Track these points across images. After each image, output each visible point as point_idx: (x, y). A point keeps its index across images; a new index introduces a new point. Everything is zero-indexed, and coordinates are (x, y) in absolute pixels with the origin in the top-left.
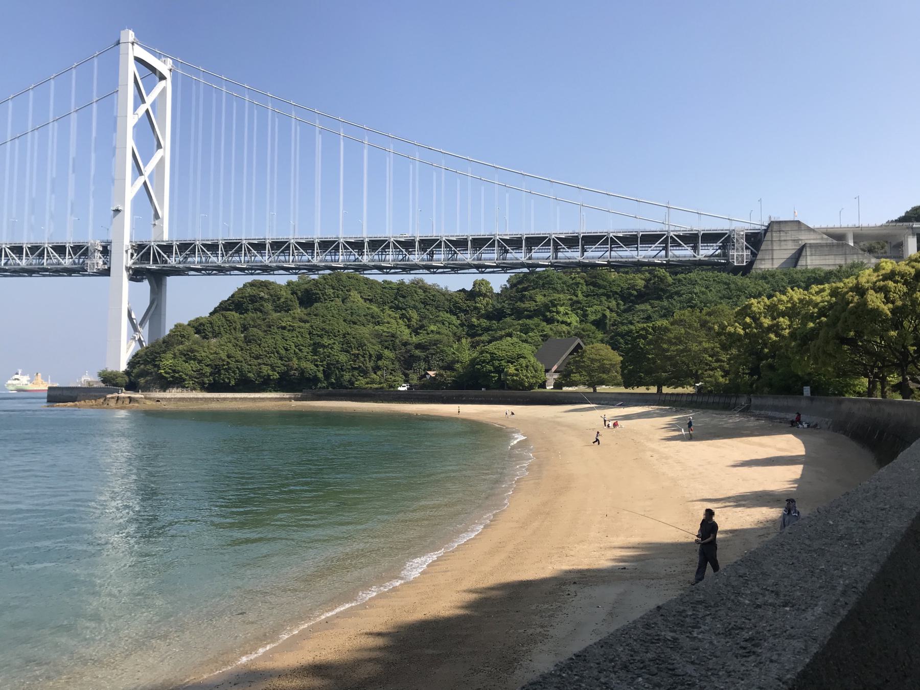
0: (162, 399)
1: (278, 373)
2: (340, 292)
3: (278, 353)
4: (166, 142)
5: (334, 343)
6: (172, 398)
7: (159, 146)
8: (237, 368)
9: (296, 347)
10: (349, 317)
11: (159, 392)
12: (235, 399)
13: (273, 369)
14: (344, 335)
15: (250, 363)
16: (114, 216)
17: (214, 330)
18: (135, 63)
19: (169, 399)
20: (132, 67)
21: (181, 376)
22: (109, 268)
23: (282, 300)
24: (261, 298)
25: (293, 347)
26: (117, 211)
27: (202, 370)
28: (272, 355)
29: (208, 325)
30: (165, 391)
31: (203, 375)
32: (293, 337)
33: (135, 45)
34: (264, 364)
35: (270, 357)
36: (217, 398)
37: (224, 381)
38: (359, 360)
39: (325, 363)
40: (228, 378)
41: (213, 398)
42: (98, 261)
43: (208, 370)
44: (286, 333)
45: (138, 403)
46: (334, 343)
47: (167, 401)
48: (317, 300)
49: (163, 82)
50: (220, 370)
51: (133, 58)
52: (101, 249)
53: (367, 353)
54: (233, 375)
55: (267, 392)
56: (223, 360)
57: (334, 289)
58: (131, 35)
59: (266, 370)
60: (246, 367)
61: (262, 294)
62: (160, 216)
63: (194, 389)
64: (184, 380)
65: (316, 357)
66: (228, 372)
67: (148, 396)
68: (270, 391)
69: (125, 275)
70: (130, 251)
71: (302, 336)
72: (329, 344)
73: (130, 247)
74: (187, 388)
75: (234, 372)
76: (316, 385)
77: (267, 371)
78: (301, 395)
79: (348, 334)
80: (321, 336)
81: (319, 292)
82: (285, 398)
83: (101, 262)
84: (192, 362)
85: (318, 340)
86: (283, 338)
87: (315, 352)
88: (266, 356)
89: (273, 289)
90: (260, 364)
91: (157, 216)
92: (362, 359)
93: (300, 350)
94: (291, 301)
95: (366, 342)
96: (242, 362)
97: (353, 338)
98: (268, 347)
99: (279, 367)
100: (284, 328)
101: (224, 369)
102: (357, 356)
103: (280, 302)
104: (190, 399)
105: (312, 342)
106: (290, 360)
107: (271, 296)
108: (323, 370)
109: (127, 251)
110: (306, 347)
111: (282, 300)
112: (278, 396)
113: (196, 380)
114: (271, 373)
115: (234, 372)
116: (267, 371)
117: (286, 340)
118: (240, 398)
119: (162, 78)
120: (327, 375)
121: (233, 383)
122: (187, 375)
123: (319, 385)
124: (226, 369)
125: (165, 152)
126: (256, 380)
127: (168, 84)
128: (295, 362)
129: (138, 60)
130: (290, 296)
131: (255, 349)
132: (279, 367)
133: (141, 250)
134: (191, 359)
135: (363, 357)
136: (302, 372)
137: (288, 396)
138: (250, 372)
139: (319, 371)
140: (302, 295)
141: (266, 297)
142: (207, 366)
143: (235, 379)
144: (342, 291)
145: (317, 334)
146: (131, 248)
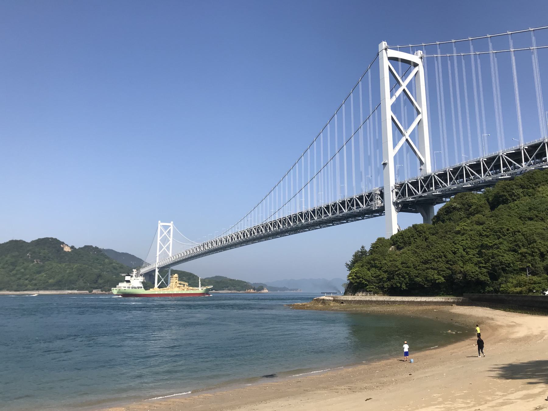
0: (345, 301)
1: (444, 277)
2: (531, 190)
3: (446, 257)
4: (424, 108)
5: (501, 243)
6: (352, 301)
7: (418, 113)
8: (406, 273)
9: (464, 250)
10: (528, 214)
11: (351, 295)
12: (403, 302)
13: (439, 274)
14: (514, 232)
15: (418, 268)
16: (384, 169)
17: (404, 240)
18: (389, 61)
19: (351, 302)
20: (386, 64)
21: (361, 281)
22: (384, 205)
23: (473, 207)
24: (454, 208)
25: (461, 250)
26: (385, 164)
27: (380, 275)
28: (440, 260)
29: (400, 237)
30: (354, 295)
31: (381, 280)
32: (463, 240)
33: (388, 49)
34: (432, 268)
35: (438, 261)
36: (387, 301)
37: (396, 285)
38: (526, 259)
39: (488, 264)
40: (399, 283)
41: (385, 301)
42: (378, 203)
43: (385, 276)
44: (460, 237)
45: (325, 304)
46: (501, 243)
47: (348, 303)
48: (505, 202)
49: (417, 68)
50: (394, 276)
51: (387, 59)
52: (380, 193)
53: (537, 250)
54: (403, 279)
55: (440, 296)
56: (397, 267)
57: (523, 188)
58: (384, 44)
59: (433, 275)
60: (414, 272)
61: (455, 204)
62: (424, 163)
63: (375, 293)
64: (367, 285)
65: (479, 259)
66: (399, 277)
67: (336, 298)
68: (443, 295)
69: (393, 208)
70: (396, 190)
71: (471, 238)
72: (495, 244)
73: (394, 188)
74: (370, 291)
75: (403, 277)
76: (484, 289)
77: (433, 275)
78: (463, 300)
79: (519, 232)
80: (487, 237)
81: (505, 194)
82: (449, 302)
83: (379, 202)
84: (373, 269)
85: (487, 241)
86: (453, 242)
87: (480, 254)
88: (435, 261)
89: (466, 199)
90: (427, 269)
91: (422, 163)
92: (530, 258)
93: (467, 253)
94: (481, 207)
95: (537, 238)
96: (410, 267)
97: (524, 235)
98: (437, 252)
99: (444, 271)
100: (458, 232)
101: (396, 275)
102: (523, 255)
103: (471, 209)
104: (367, 302)
105: (480, 244)
106: (455, 263)
107: (464, 205)
108: (488, 272)
109: (392, 191)
110: (473, 249)
111: (473, 207)
112: (443, 300)
113: (377, 285)
114: (436, 276)
115: (403, 277)
116: (433, 275)
117: (455, 244)
118: (408, 302)
119: (416, 65)
120: (494, 276)
121: (404, 287)
122: (366, 280)
123: (487, 289)
124: (398, 274)
125: (424, 116)
126: (425, 284)
127: (421, 69)
128: (459, 267)
129: (390, 59)
130: (483, 201)
131: (427, 255)
132: (444, 271)
133: (401, 189)
134: (372, 266)
135: (533, 256)
136: (465, 275)
137: (452, 300)
138: (417, 277)
139: (482, 274)
140: (492, 200)
141: (458, 206)
142: (385, 272)
143: (406, 284)
144: (533, 188)
145: (486, 235)
146: (395, 188)
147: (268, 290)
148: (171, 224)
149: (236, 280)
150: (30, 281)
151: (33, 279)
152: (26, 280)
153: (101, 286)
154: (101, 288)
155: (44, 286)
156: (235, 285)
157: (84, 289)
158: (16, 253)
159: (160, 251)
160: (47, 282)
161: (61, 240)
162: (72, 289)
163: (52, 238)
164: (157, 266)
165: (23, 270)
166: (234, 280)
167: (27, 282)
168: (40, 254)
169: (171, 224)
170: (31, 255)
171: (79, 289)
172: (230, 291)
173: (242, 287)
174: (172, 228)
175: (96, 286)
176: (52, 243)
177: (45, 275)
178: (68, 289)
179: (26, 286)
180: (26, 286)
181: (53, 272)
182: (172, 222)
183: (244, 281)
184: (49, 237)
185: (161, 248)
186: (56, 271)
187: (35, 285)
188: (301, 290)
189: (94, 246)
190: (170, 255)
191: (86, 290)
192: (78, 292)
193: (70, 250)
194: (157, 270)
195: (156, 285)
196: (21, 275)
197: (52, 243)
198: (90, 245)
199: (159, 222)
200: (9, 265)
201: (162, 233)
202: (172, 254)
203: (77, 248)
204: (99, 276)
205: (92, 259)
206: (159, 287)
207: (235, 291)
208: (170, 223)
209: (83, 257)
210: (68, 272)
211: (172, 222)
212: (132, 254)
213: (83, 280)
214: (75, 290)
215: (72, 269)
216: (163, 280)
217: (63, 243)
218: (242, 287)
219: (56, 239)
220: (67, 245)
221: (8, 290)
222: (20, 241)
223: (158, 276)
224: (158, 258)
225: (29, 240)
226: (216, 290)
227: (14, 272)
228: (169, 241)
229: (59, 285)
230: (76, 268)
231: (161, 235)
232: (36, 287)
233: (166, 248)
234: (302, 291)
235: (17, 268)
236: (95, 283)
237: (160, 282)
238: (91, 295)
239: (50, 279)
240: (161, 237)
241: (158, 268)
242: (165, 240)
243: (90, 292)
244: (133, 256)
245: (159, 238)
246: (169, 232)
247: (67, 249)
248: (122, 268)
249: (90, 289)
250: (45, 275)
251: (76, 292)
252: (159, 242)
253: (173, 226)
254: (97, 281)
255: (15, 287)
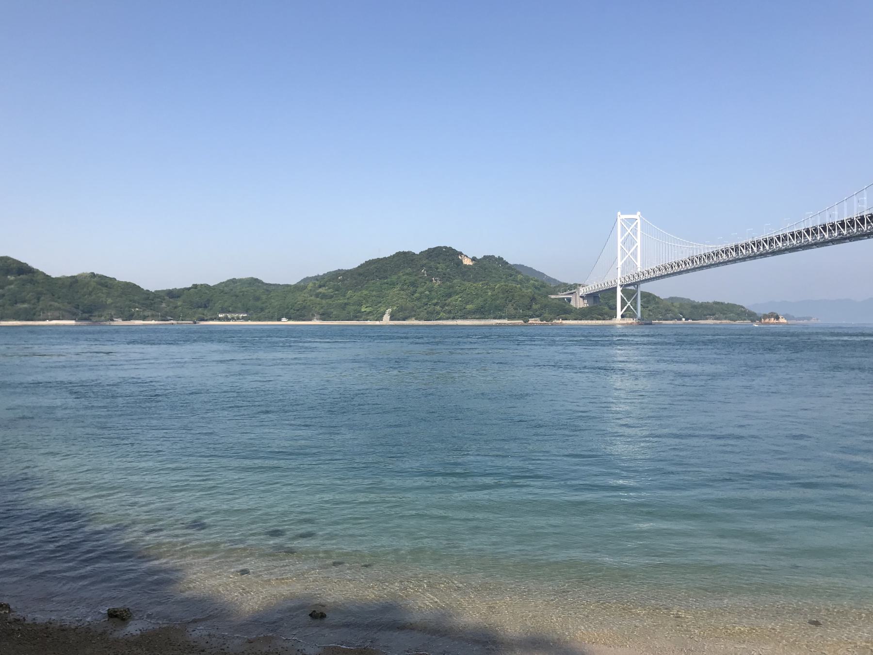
147: (786, 319)
148: (637, 216)
149: (726, 303)
150: (442, 307)
151: (445, 304)
152: (435, 305)
153: (537, 313)
154: (538, 316)
155: (462, 314)
156: (726, 312)
157: (515, 318)
158: (409, 270)
159: (622, 259)
160: (464, 308)
161: (458, 250)
162: (500, 318)
163: (445, 247)
164: (619, 283)
165: (427, 292)
166: (722, 303)
167: (438, 308)
168: (438, 270)
169: (637, 216)
170: (427, 271)
171: (510, 317)
172: (718, 322)
173: (738, 314)
174: (639, 221)
175: (531, 313)
176: (448, 254)
177: (460, 299)
178: (495, 318)
179: (438, 313)
180: (438, 313)
181: (469, 294)
182: (639, 213)
183: (739, 306)
184: (442, 245)
185: (624, 254)
186: (471, 292)
187: (450, 312)
188: (817, 319)
189: (497, 256)
190: (639, 264)
191: (519, 318)
192: (509, 322)
193: (471, 264)
194: (619, 289)
195: (619, 313)
196: (427, 300)
197: (448, 254)
198: (491, 255)
199: (619, 213)
200: (408, 286)
201: (624, 230)
202: (642, 265)
203: (479, 257)
204: (533, 299)
205: (504, 275)
206: (623, 316)
207: (728, 321)
208: (636, 214)
209: (491, 272)
210: (490, 294)
211: (639, 213)
212: (529, 266)
213: (513, 305)
214: (504, 318)
215: (493, 289)
216: (629, 304)
217: (461, 254)
218: (738, 314)
219: (450, 248)
220: (467, 257)
221: (416, 319)
222: (409, 252)
223: (622, 299)
224: (619, 270)
225: (417, 252)
226: (693, 320)
227: (417, 295)
228: (633, 243)
229: (481, 312)
230: (499, 288)
231: (622, 235)
232: (452, 315)
233: (631, 254)
234: (819, 321)
235: (420, 290)
236: (528, 309)
237: (626, 307)
238: (526, 326)
239: (467, 303)
240: (623, 238)
241: (621, 286)
242: (629, 242)
243: (525, 322)
244: (531, 269)
245: (620, 240)
246: (636, 226)
247: (467, 262)
248: (545, 287)
249: (526, 318)
250: (460, 299)
251: (506, 321)
252: (620, 245)
253: (641, 219)
254: (531, 306)
255: (424, 314)
